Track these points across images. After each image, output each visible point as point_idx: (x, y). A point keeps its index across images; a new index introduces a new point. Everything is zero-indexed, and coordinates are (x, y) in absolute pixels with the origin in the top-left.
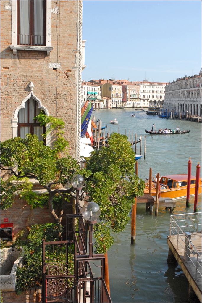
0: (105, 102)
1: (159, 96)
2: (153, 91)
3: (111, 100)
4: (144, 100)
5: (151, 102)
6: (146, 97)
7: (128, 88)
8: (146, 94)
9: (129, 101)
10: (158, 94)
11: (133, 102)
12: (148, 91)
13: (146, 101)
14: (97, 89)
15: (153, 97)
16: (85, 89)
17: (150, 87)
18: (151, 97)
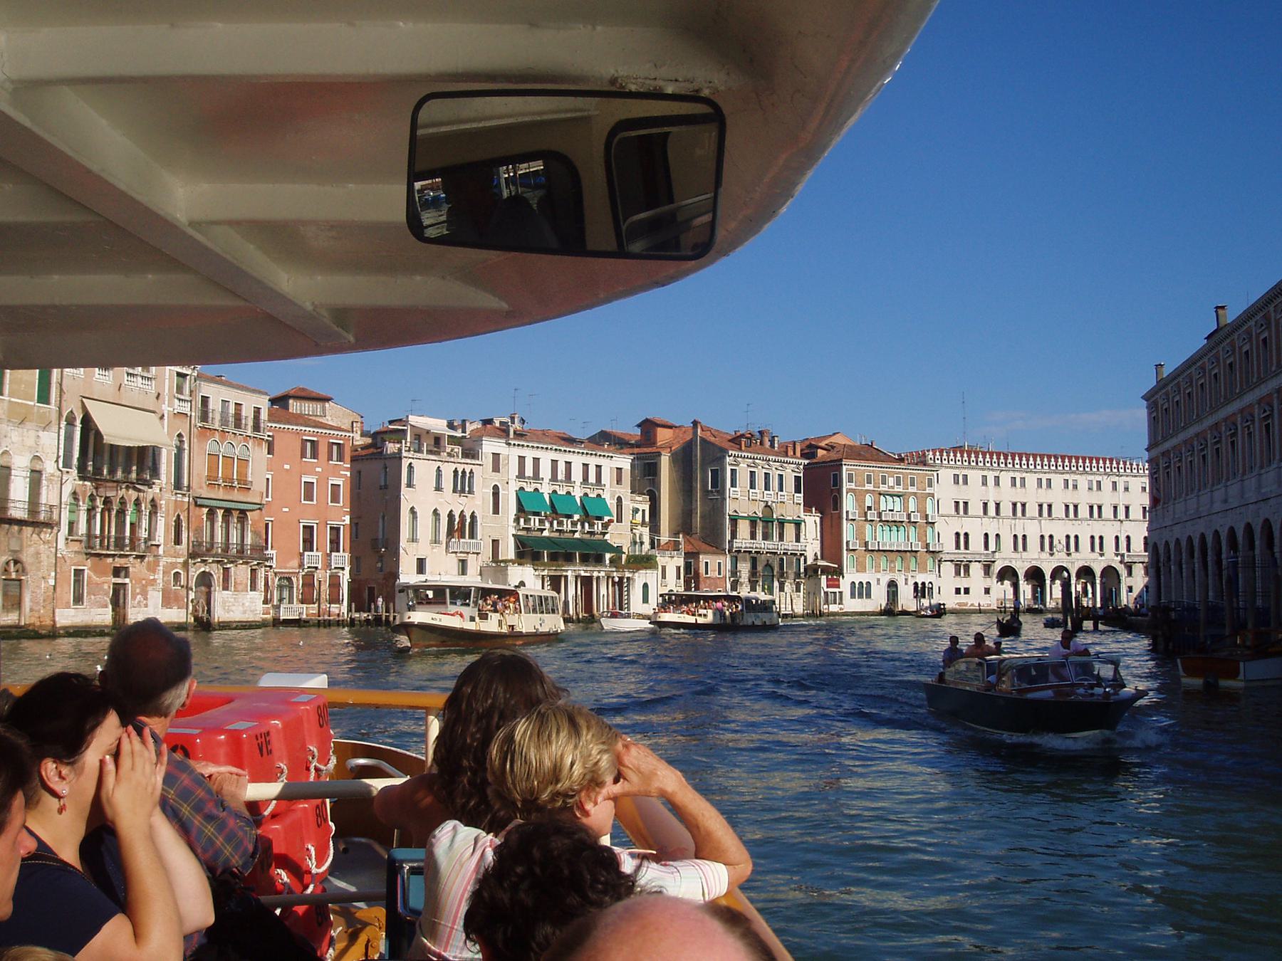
0: (671, 573)
1: (1059, 538)
2: (1019, 509)
3: (720, 559)
4: (962, 568)
5: (1008, 574)
6: (976, 544)
7: (850, 481)
8: (975, 527)
9: (861, 568)
10: (1048, 528)
11: (885, 580)
12: (985, 505)
13: (976, 569)
14: (606, 478)
15: (1020, 543)
16: (496, 468)
17: (997, 478)
18: (1007, 542)
